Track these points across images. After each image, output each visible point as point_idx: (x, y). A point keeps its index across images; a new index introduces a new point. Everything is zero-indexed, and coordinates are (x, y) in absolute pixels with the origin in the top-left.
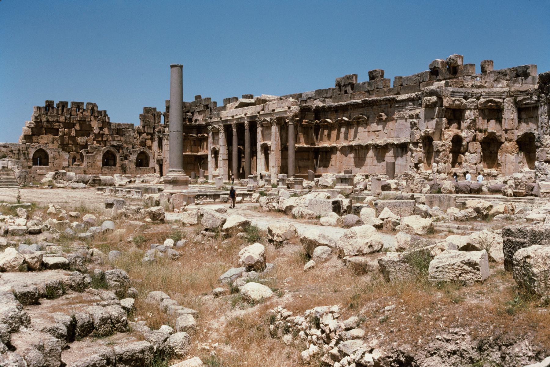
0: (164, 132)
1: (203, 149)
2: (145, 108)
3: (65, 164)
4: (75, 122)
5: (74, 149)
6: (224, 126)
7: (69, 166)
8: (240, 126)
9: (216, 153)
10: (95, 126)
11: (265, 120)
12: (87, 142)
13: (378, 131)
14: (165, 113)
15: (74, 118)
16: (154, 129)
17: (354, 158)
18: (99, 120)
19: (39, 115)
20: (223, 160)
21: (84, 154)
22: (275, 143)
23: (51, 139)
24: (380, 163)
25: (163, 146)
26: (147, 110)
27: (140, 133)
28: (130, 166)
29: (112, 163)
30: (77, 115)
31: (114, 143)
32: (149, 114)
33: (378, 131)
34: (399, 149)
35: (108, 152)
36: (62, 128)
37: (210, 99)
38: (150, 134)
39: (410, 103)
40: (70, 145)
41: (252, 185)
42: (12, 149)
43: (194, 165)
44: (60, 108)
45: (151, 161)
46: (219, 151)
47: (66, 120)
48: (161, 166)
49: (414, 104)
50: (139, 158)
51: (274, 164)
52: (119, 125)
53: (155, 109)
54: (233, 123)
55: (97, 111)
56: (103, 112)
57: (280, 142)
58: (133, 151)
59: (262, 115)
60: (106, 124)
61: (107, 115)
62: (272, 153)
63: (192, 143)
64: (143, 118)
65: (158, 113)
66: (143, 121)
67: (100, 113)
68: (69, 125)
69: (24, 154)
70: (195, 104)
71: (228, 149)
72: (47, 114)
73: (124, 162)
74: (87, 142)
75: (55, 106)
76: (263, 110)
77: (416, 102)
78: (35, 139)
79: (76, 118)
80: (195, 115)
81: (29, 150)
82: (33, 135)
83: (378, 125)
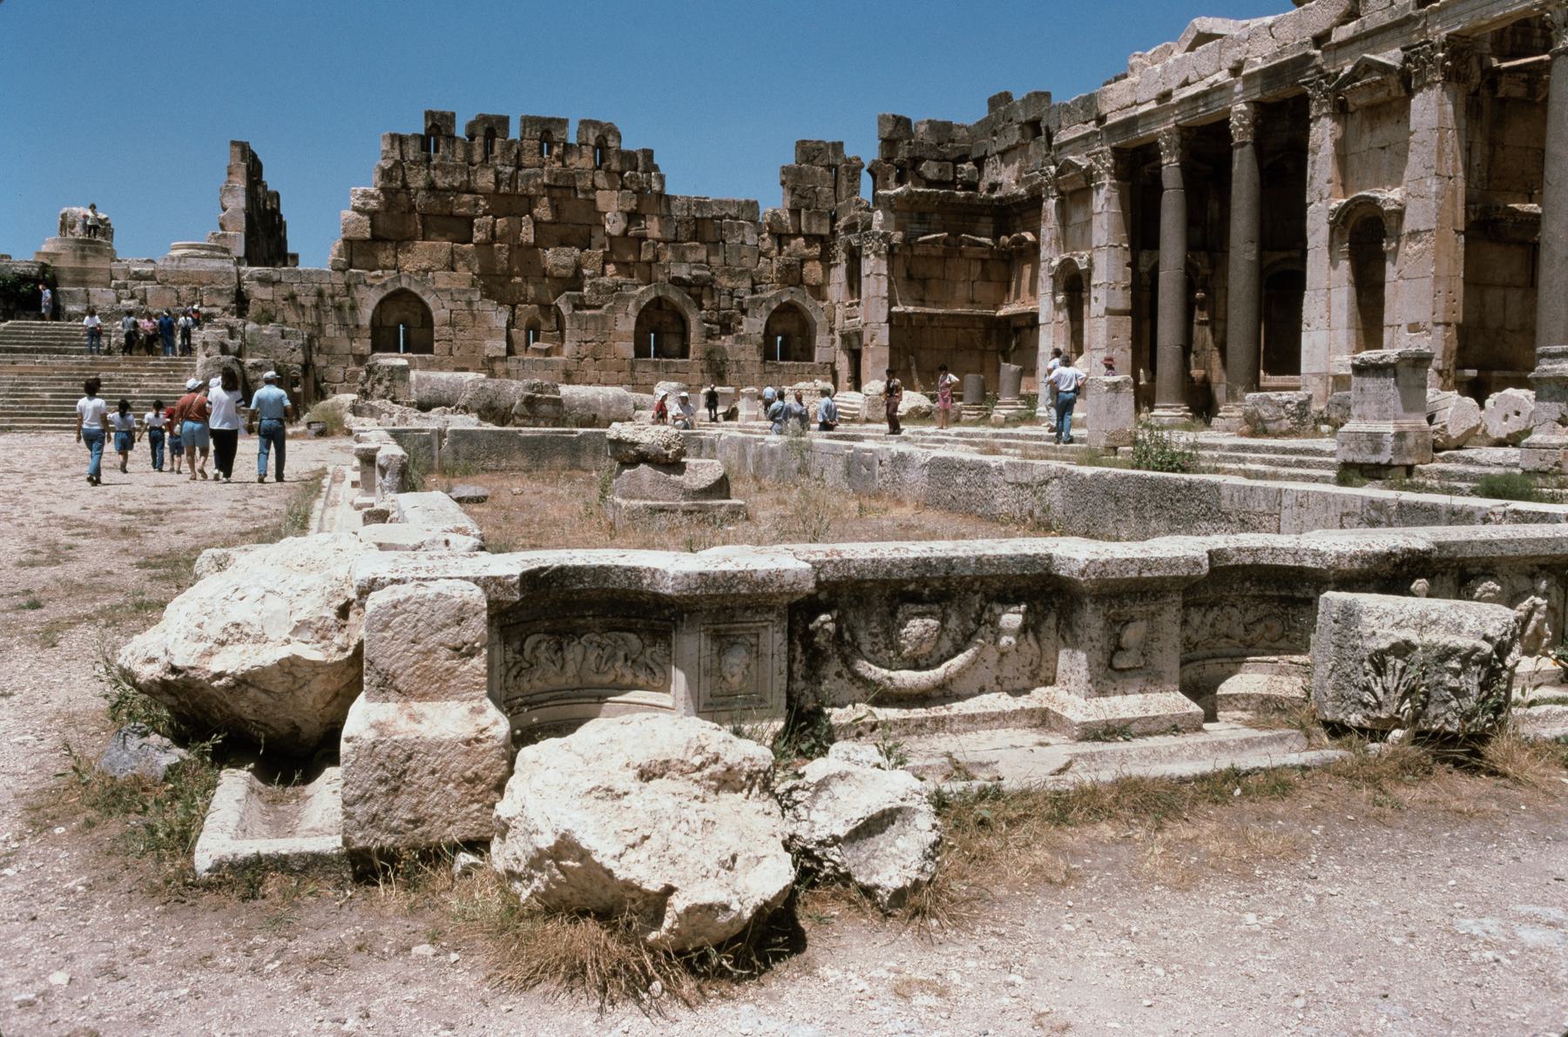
0: (869, 226)
1: (1017, 296)
2: (802, 145)
3: (496, 346)
4: (532, 190)
5: (531, 290)
6: (1117, 152)
7: (510, 351)
8: (1205, 143)
9: (1074, 285)
10: (612, 208)
11: (1370, 67)
12: (578, 267)
14: (875, 163)
15: (528, 176)
16: (834, 219)
18: (623, 187)
19: (397, 164)
20: (1110, 312)
21: (566, 310)
22: (1433, 186)
23: (443, 255)
25: (864, 280)
26: (809, 152)
27: (781, 238)
28: (742, 356)
29: (675, 345)
30: (541, 167)
31: (683, 272)
32: (816, 169)
35: (658, 303)
36: (486, 214)
37: (1047, 95)
38: (821, 239)
40: (518, 279)
41: (1389, 428)
42: (295, 288)
43: (983, 353)
44: (479, 140)
45: (821, 339)
46: (1089, 272)
47: (498, 182)
48: (855, 357)
50: (778, 327)
51: (1423, 315)
52: (701, 204)
53: (838, 147)
54: (1163, 129)
55: (619, 152)
56: (640, 157)
57: (1461, 184)
58: (753, 301)
59: (1340, 45)
60: (649, 200)
61: (656, 168)
62: (1410, 249)
63: (976, 269)
64: (793, 179)
65: (849, 161)
66: (793, 190)
67: (629, 158)
68: (511, 203)
69: (339, 308)
70: (989, 127)
71: (1133, 265)
72: (429, 159)
73: (718, 343)
74: (578, 267)
75: (460, 131)
78: (385, 257)
79: (536, 175)
80: (987, 170)
81: (357, 296)
82: (375, 238)
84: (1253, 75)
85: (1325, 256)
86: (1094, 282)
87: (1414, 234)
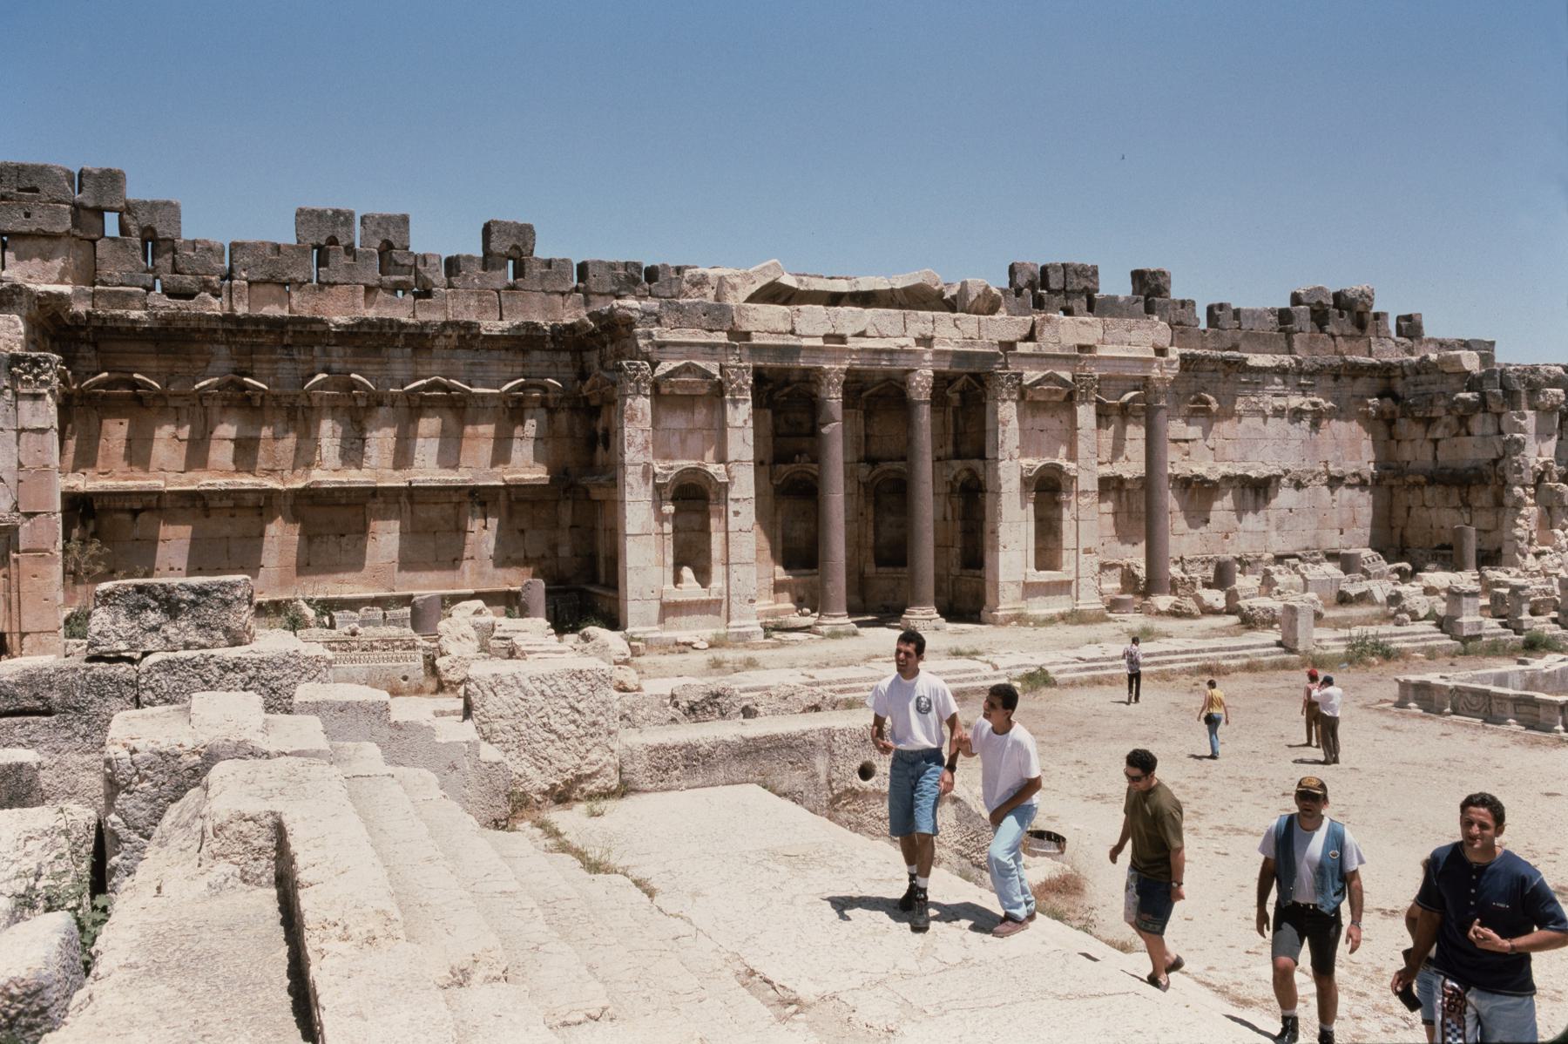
6: (759, 375)
8: (877, 393)
13: (1186, 441)
17: (1115, 514)
24: (1197, 528)
33: (1186, 441)
34: (1248, 492)
39: (1277, 380)
49: (1285, 383)
76: (1030, 337)
77: (1290, 379)
83: (1188, 424)
84: (945, 352)
85: (1017, 498)
86: (731, 495)
87: (1085, 492)
